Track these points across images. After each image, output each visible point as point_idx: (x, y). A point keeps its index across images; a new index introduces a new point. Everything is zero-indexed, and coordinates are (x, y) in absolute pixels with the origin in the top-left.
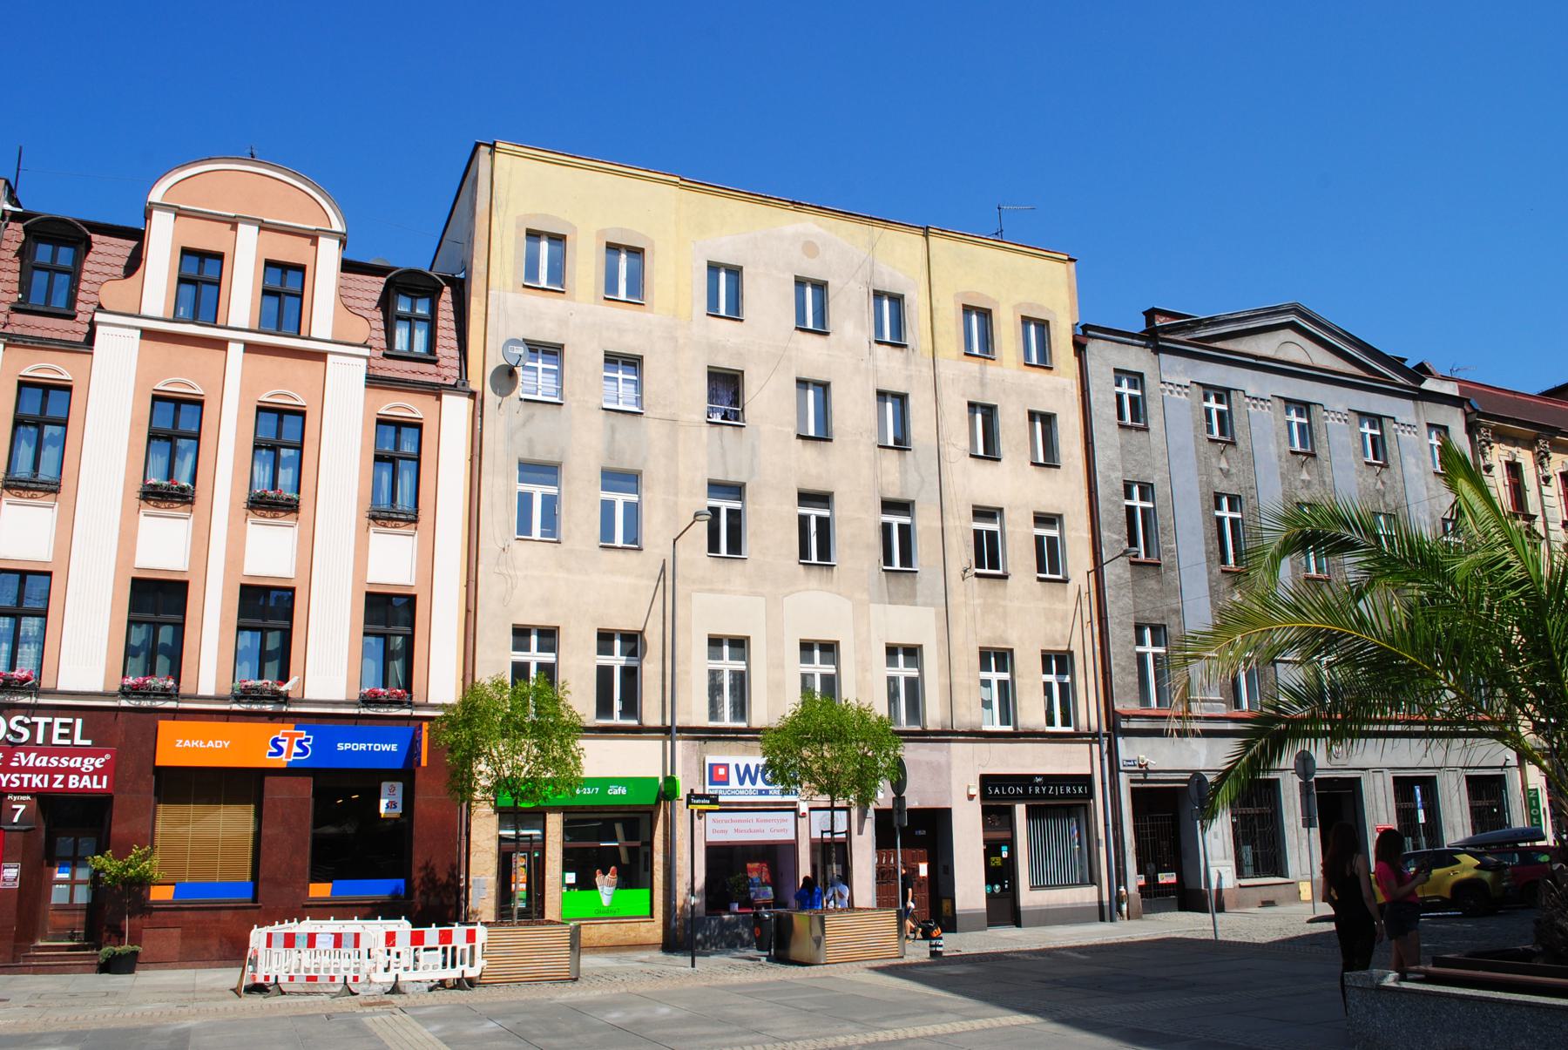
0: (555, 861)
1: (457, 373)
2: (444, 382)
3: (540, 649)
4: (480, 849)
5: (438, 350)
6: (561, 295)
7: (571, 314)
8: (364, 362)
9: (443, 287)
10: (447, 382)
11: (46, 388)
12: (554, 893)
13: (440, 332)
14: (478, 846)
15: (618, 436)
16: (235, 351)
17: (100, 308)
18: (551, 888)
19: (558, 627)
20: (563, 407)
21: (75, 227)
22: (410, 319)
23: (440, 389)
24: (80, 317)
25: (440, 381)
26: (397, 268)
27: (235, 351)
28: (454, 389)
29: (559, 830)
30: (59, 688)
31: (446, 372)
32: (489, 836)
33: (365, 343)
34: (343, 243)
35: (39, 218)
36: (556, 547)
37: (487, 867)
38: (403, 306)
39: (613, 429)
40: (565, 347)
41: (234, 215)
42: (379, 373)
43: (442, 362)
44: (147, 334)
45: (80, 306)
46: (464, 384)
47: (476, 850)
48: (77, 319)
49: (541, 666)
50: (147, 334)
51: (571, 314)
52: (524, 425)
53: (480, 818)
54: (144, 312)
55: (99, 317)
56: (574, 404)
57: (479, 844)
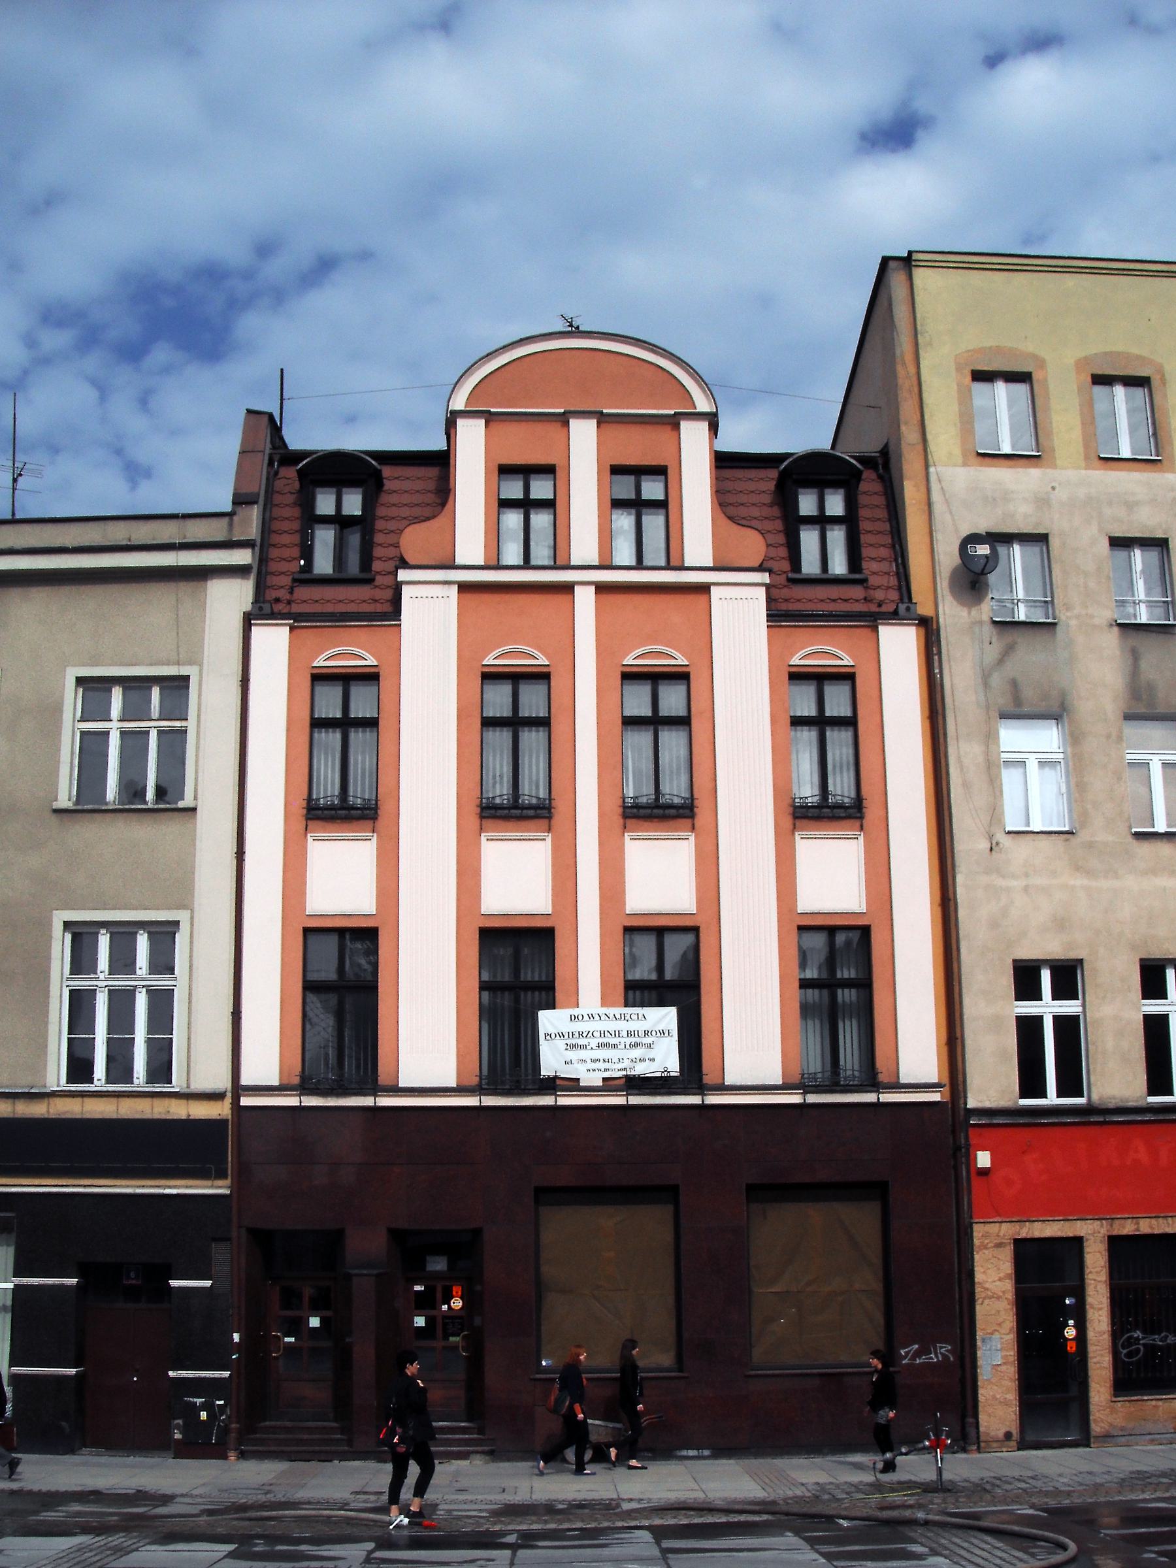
0: (1100, 1309)
1: (894, 595)
2: (877, 610)
3: (1055, 997)
4: (989, 1293)
5: (864, 565)
6: (1035, 460)
7: (1053, 488)
8: (762, 592)
9: (860, 473)
10: (884, 609)
11: (346, 679)
12: (1102, 1355)
13: (864, 539)
14: (987, 1289)
15: (1144, 665)
16: (585, 599)
17: (405, 564)
18: (1095, 1348)
19: (1081, 961)
20: (1058, 628)
21: (359, 457)
22: (822, 521)
23: (875, 620)
24: (379, 580)
25: (873, 608)
26: (792, 454)
27: (585, 599)
28: (894, 617)
29: (1103, 1264)
30: (401, 1085)
31: (879, 595)
32: (1002, 1275)
33: (761, 565)
34: (714, 428)
35: (315, 456)
36: (1067, 840)
37: (1001, 1320)
38: (807, 504)
39: (1135, 655)
40: (1050, 538)
41: (562, 411)
42: (784, 607)
43: (873, 581)
44: (465, 588)
45: (377, 566)
46: (908, 609)
47: (983, 1295)
48: (377, 583)
49: (1059, 1020)
50: (465, 588)
51: (1053, 488)
52: (1001, 661)
53: (986, 1248)
54: (459, 561)
55: (403, 575)
56: (1073, 622)
57: (987, 1285)
